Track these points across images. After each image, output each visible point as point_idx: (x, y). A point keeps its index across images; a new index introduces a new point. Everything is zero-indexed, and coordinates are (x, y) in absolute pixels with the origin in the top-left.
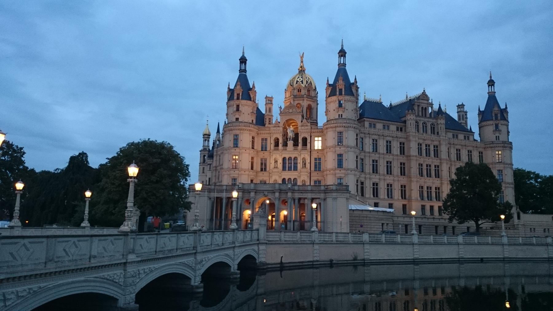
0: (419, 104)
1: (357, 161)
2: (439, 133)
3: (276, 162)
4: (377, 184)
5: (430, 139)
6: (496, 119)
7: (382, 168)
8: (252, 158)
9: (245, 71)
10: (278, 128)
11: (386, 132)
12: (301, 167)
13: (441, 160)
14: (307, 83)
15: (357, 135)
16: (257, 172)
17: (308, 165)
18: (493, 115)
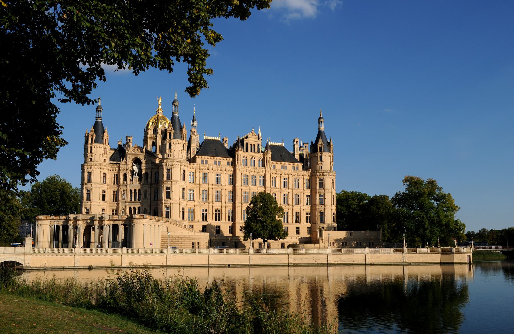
0: (247, 142)
1: (183, 193)
2: (266, 165)
4: (206, 210)
5: (259, 171)
6: (321, 151)
7: (212, 197)
8: (104, 192)
10: (126, 166)
11: (217, 167)
12: (144, 198)
13: (265, 188)
14: (161, 124)
16: (110, 203)
17: (149, 197)
18: (319, 148)
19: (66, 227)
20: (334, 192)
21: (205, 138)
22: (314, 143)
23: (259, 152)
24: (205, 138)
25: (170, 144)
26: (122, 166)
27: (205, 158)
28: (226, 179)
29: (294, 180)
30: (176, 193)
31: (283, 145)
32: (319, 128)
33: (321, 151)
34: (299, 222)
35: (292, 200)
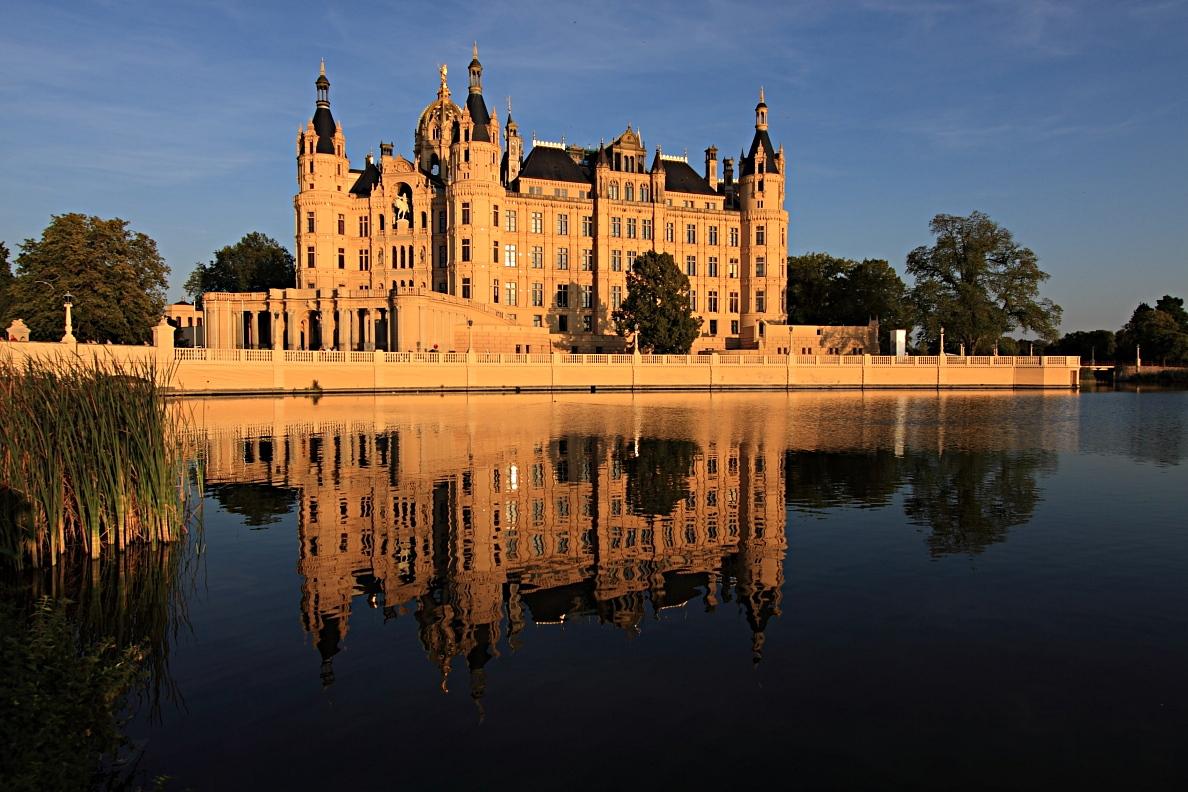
0: (618, 150)
2: (654, 197)
3: (381, 254)
6: (761, 171)
8: (341, 250)
9: (328, 103)
15: (496, 207)
16: (354, 272)
18: (757, 166)
19: (265, 317)
20: (784, 254)
21: (535, 144)
22: (746, 156)
23: (641, 171)
24: (535, 145)
25: (467, 153)
26: (375, 200)
27: (536, 182)
28: (577, 225)
29: (708, 229)
30: (481, 251)
31: (686, 162)
32: (757, 127)
33: (761, 171)
34: (715, 310)
35: (702, 267)
